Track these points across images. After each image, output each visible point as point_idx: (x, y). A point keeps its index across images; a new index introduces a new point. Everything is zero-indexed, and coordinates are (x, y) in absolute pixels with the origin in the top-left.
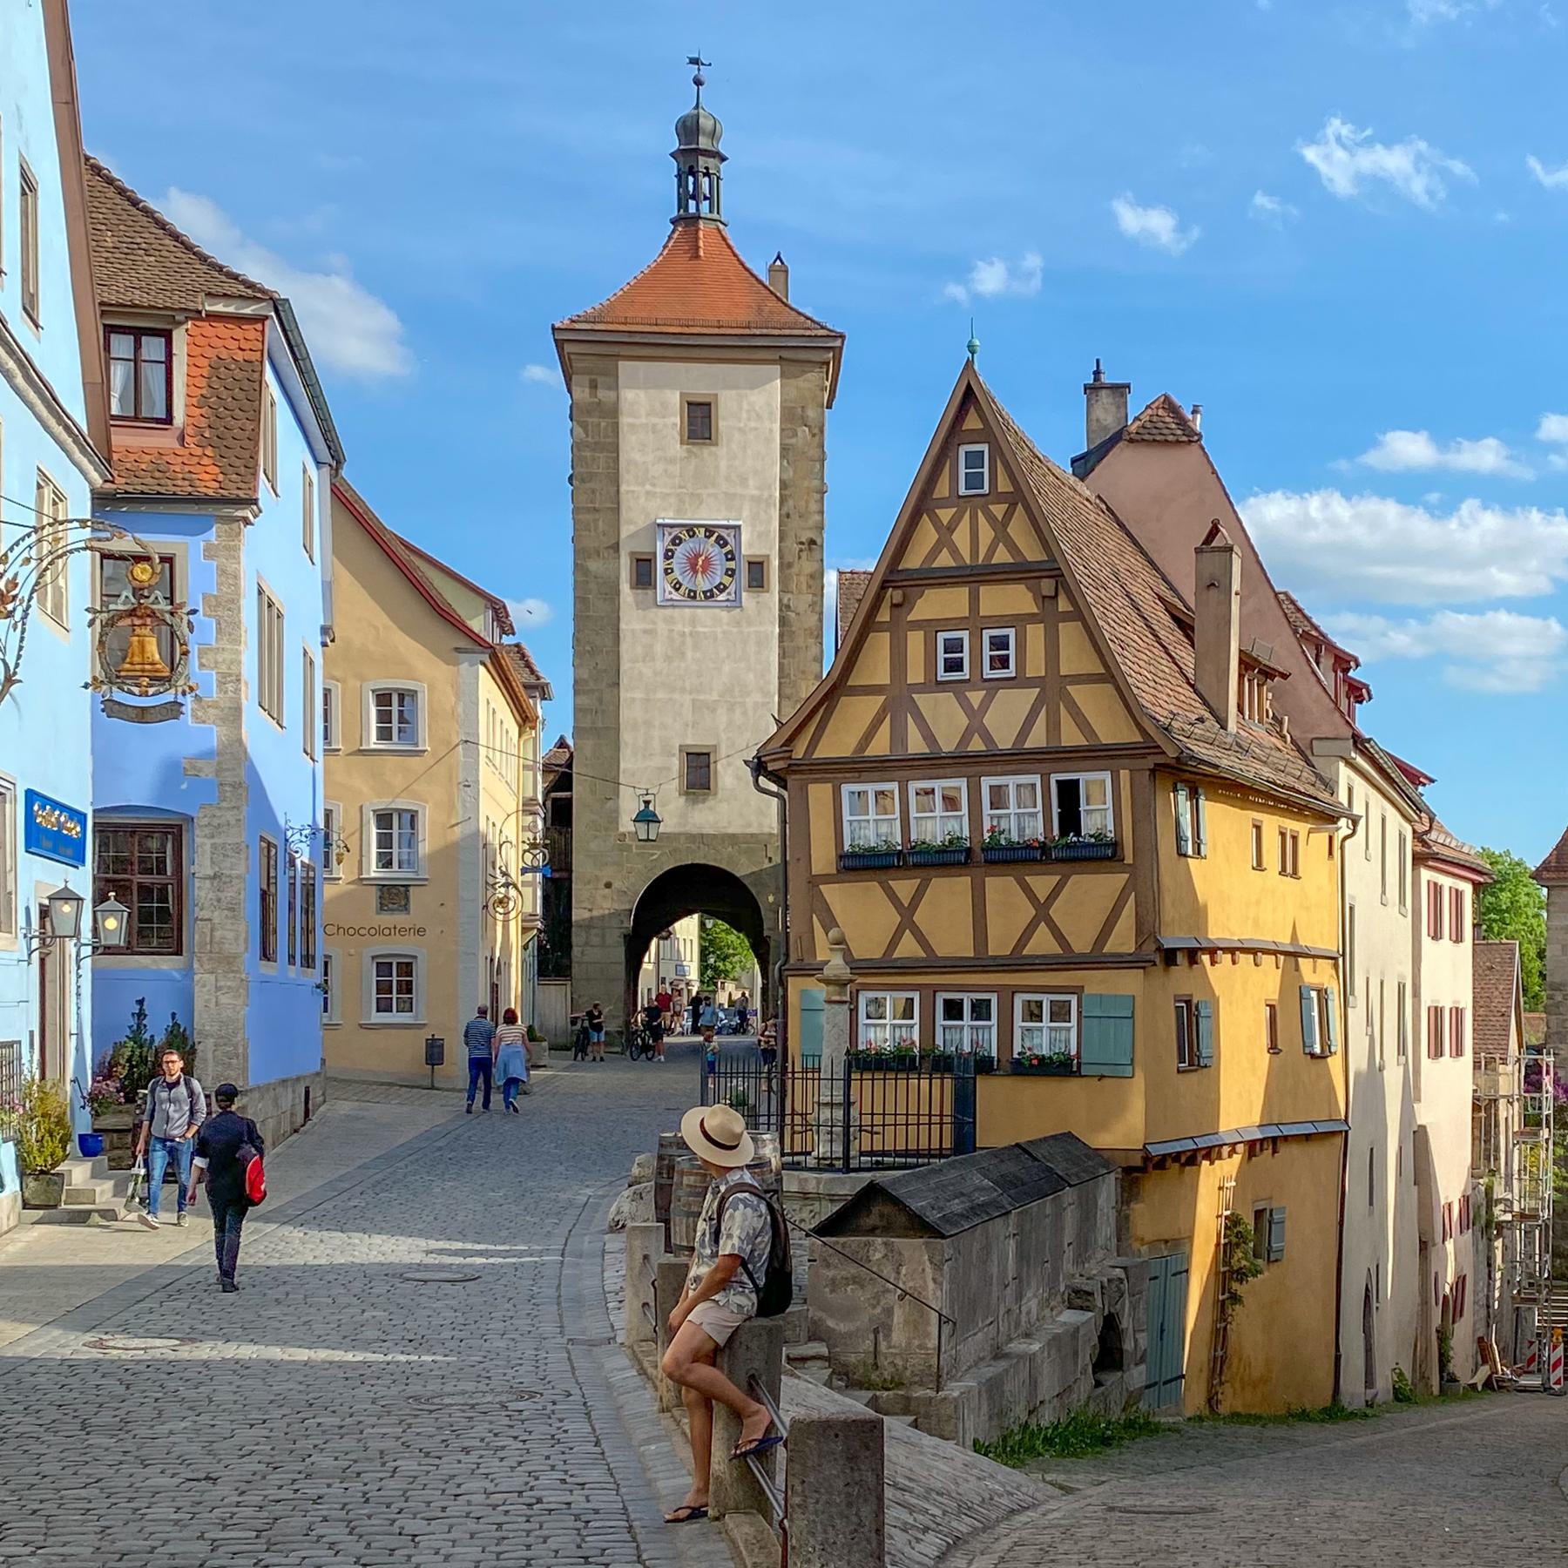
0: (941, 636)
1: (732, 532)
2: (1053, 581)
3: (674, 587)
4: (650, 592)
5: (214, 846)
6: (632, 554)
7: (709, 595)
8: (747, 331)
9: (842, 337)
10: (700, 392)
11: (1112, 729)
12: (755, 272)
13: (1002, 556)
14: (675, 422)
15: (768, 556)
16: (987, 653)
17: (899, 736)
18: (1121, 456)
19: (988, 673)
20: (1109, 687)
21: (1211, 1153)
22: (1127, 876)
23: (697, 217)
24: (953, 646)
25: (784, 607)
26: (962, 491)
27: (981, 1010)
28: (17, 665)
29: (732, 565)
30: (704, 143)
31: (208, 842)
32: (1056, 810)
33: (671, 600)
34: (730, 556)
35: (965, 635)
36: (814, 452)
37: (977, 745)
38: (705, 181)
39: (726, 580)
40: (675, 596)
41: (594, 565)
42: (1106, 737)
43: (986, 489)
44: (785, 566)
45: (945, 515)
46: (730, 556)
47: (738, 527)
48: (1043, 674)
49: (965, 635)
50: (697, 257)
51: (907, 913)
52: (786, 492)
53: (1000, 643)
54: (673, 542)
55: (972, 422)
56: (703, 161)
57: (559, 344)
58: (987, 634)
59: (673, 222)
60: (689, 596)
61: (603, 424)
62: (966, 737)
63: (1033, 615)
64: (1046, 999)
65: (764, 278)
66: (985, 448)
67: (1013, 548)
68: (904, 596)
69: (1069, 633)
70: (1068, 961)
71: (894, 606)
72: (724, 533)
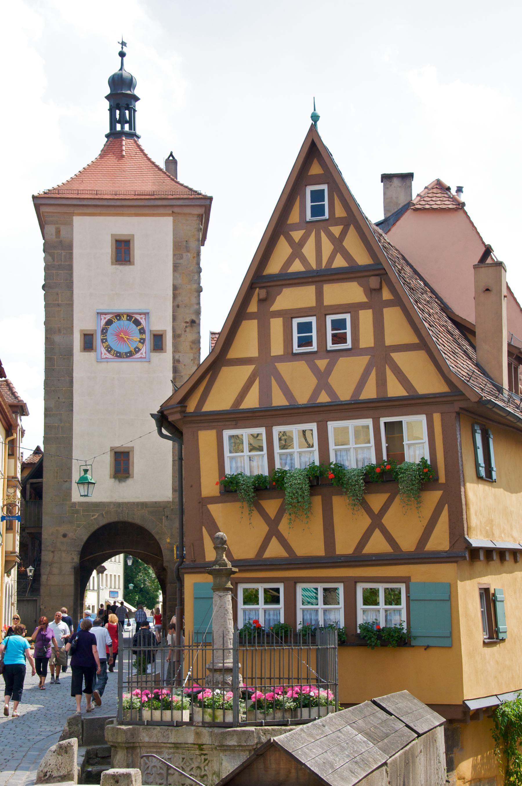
1: (142, 316)
2: (378, 279)
3: (107, 350)
4: (92, 355)
6: (81, 331)
7: (130, 355)
8: (153, 197)
9: (211, 199)
12: (157, 164)
13: (340, 262)
15: (165, 331)
16: (330, 332)
19: (330, 346)
20: (421, 355)
23: (122, 133)
24: (305, 328)
25: (176, 361)
26: (309, 217)
29: (144, 336)
32: (384, 445)
33: (106, 358)
34: (142, 331)
35: (313, 320)
37: (324, 398)
39: (140, 346)
40: (109, 356)
41: (57, 338)
43: (327, 216)
44: (176, 336)
45: (297, 235)
46: (142, 331)
47: (146, 314)
48: (372, 345)
49: (313, 320)
50: (123, 156)
52: (177, 292)
53: (339, 325)
55: (316, 169)
57: (37, 207)
58: (329, 319)
60: (117, 356)
61: (63, 254)
62: (316, 393)
63: (365, 303)
64: (381, 587)
65: (162, 166)
66: (325, 187)
67: (347, 256)
68: (267, 293)
71: (261, 301)
72: (138, 317)
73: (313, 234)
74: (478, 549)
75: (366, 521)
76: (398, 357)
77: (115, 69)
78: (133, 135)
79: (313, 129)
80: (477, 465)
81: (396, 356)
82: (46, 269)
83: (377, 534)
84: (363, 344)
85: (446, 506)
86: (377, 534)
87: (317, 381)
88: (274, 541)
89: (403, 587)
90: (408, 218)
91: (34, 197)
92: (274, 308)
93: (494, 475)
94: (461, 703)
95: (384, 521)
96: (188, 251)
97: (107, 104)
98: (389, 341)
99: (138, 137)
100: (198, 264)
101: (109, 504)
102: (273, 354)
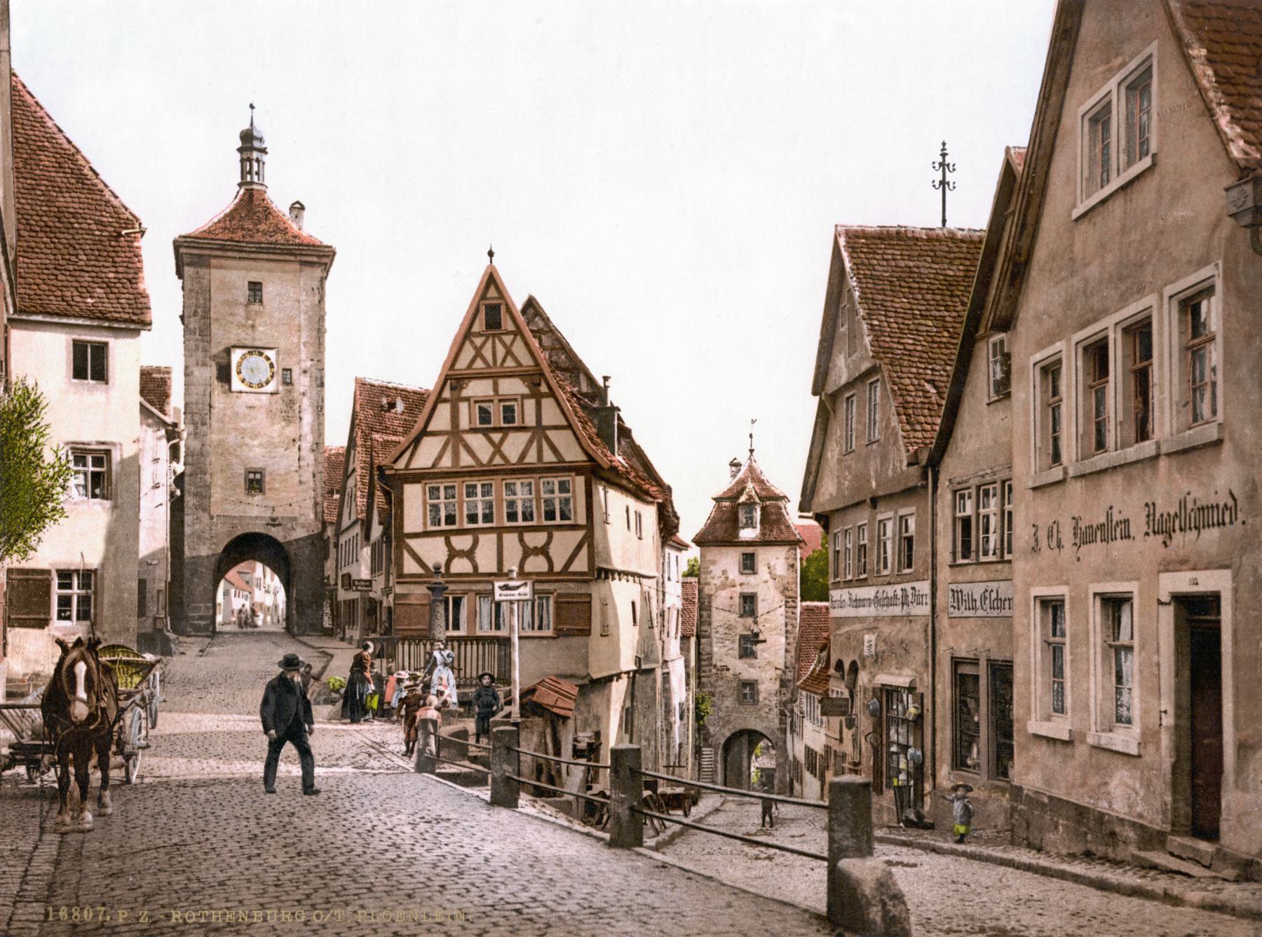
10: (254, 276)
13: (510, 363)
17: (456, 455)
20: (570, 432)
21: (619, 676)
30: (256, 144)
37: (498, 460)
38: (255, 165)
42: (568, 457)
45: (478, 341)
55: (492, 293)
56: (255, 155)
67: (515, 359)
71: (452, 389)
77: (247, 126)
97: (238, 156)
98: (545, 422)
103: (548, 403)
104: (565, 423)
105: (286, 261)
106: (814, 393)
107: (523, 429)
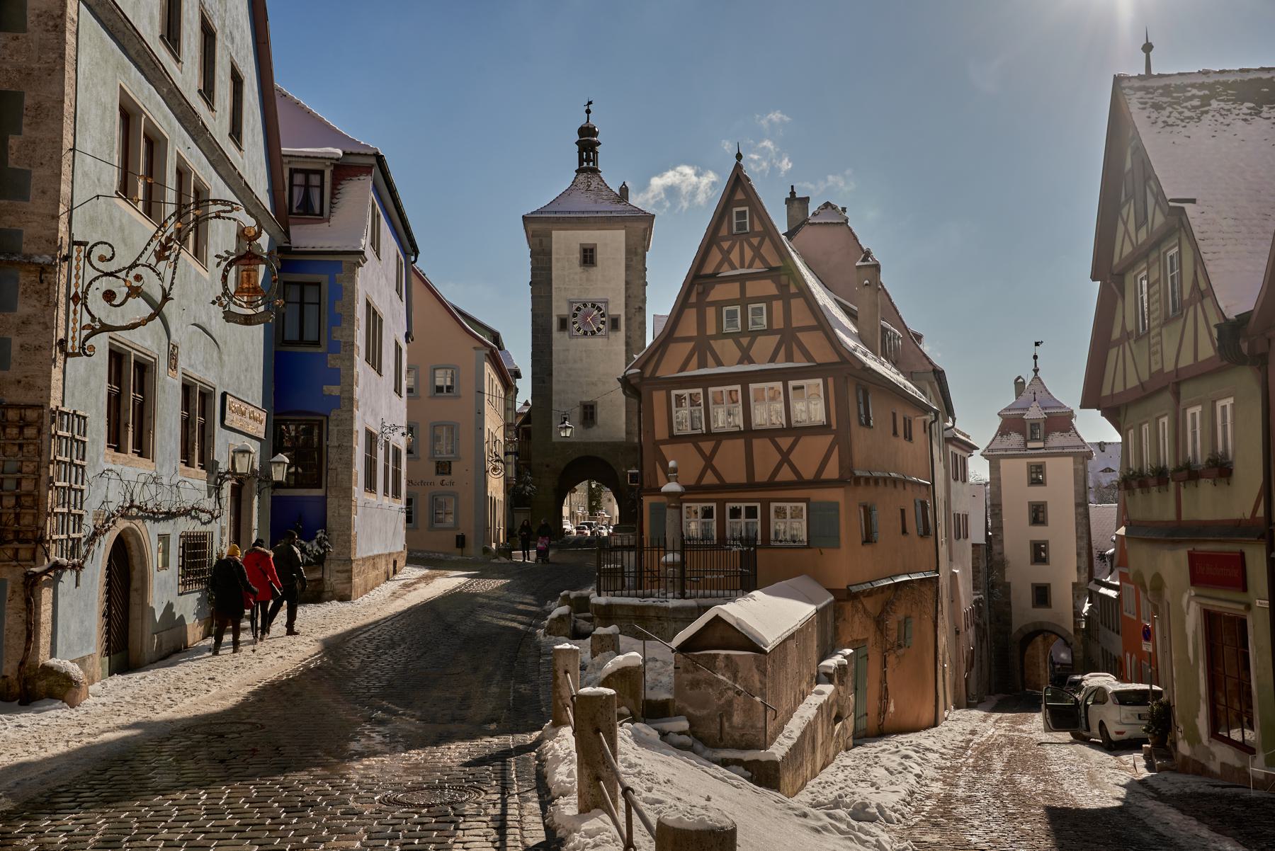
0: (725, 309)
4: (567, 333)
5: (338, 431)
6: (558, 316)
7: (593, 333)
11: (823, 354)
13: (758, 268)
14: (577, 256)
18: (805, 233)
19: (751, 327)
20: (820, 334)
22: (833, 436)
24: (732, 315)
25: (628, 337)
26: (734, 230)
27: (751, 513)
28: (171, 289)
31: (336, 429)
35: (738, 308)
36: (641, 267)
39: (601, 326)
42: (819, 359)
44: (627, 319)
45: (726, 245)
48: (782, 327)
49: (738, 308)
51: (708, 460)
54: (577, 310)
55: (740, 196)
58: (751, 307)
59: (576, 171)
65: (618, 192)
66: (746, 209)
67: (763, 260)
68: (704, 289)
69: (797, 304)
70: (801, 483)
71: (698, 294)
72: (600, 305)
73: (738, 243)
74: (859, 478)
75: (778, 457)
76: (802, 336)
78: (595, 171)
79: (738, 167)
80: (860, 415)
81: (799, 335)
82: (532, 270)
83: (786, 467)
84: (775, 327)
85: (837, 447)
86: (786, 467)
87: (740, 354)
88: (709, 472)
89: (804, 505)
90: (806, 229)
91: (524, 217)
92: (709, 299)
93: (872, 424)
94: (845, 588)
95: (791, 457)
96: (636, 254)
98: (795, 324)
99: (600, 172)
100: (644, 265)
101: (579, 443)
102: (709, 333)
103: (797, 304)
104: (816, 323)
105: (583, 212)
106: (1094, 278)
107: (769, 331)
